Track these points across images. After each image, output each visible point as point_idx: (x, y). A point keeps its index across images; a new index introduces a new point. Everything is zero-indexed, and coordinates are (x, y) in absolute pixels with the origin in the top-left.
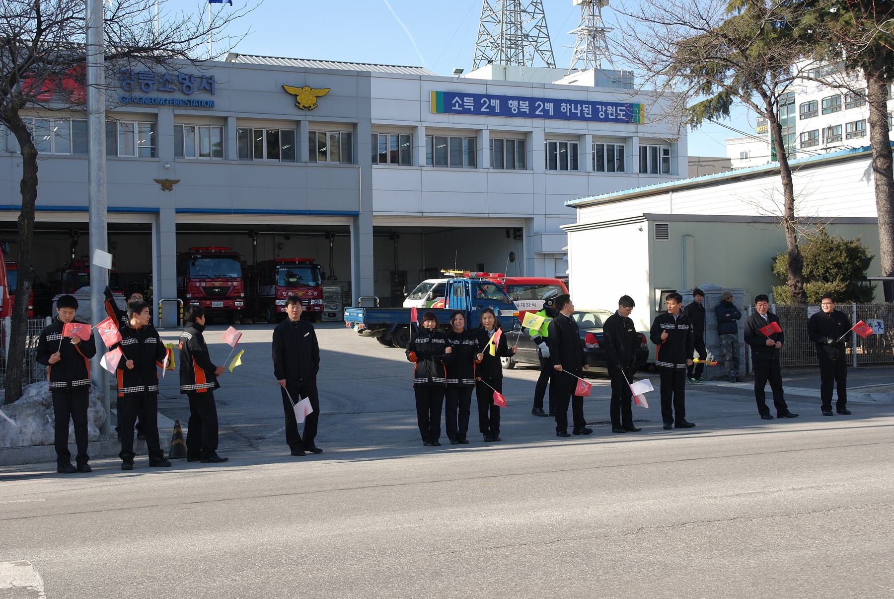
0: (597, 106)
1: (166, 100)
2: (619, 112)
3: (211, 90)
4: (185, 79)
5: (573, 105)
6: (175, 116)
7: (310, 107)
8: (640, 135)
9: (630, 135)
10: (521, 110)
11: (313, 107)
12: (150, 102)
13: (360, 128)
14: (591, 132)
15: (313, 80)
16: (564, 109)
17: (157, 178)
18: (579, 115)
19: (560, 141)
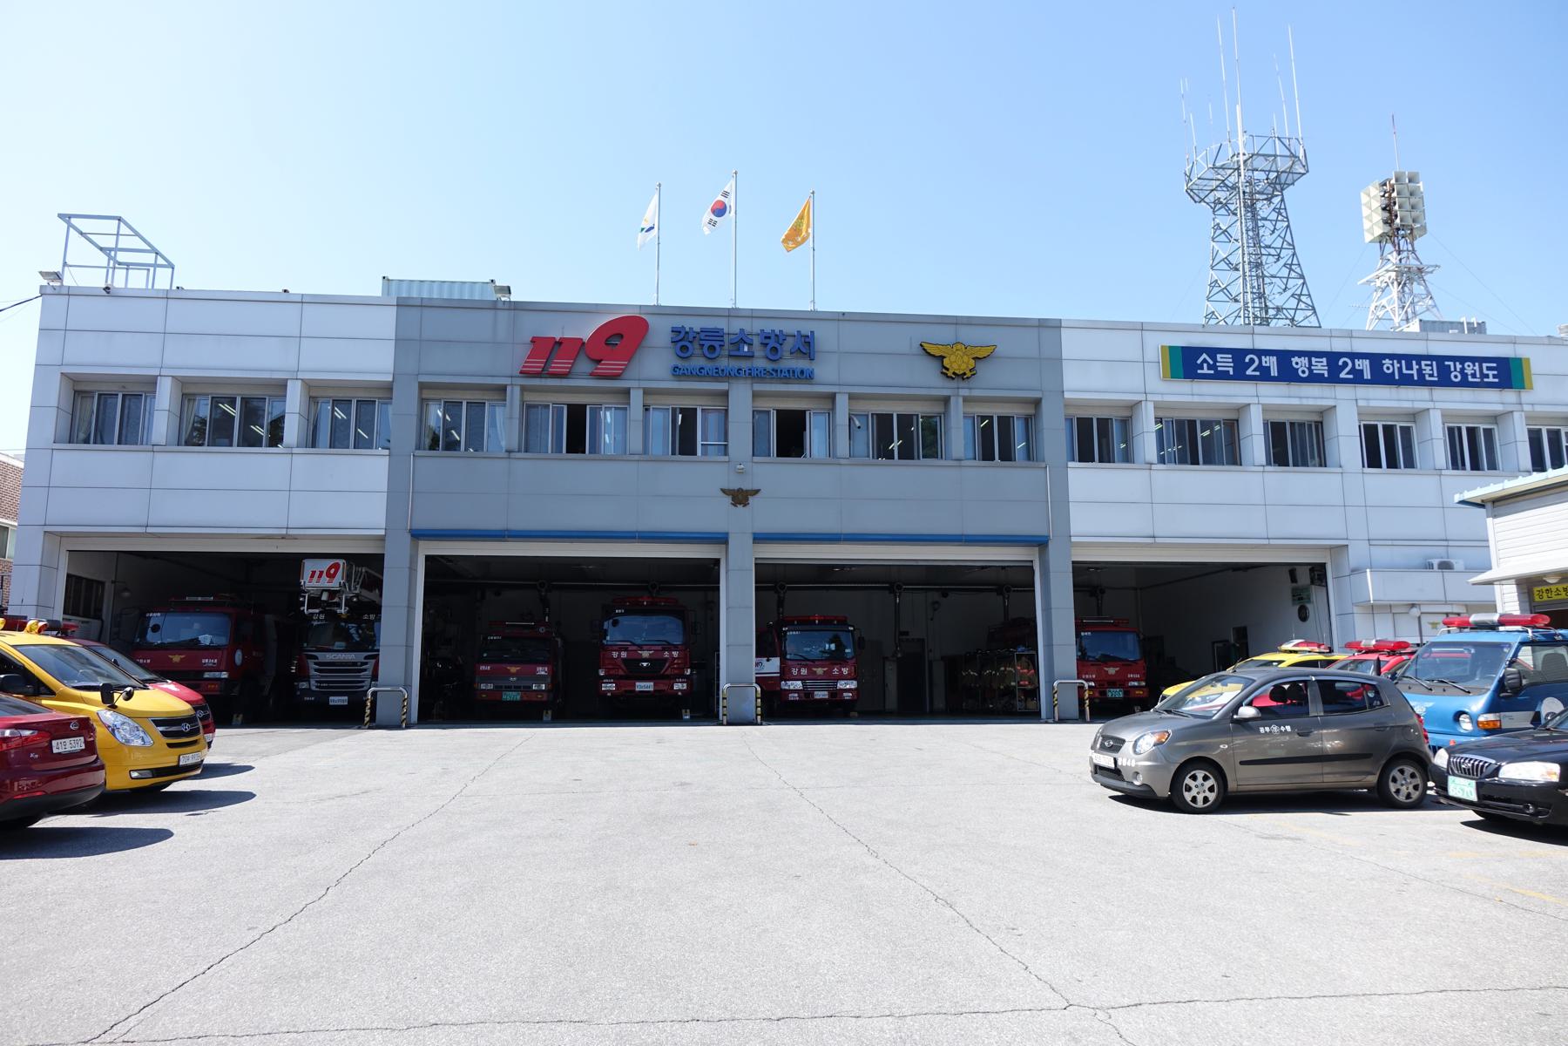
0: (1447, 363)
1: (741, 369)
4: (769, 338)
5: (1403, 362)
6: (756, 395)
7: (965, 374)
8: (1526, 408)
9: (1510, 408)
10: (1315, 372)
11: (969, 374)
12: (716, 373)
13: (1046, 407)
14: (1438, 405)
15: (969, 336)
16: (1388, 368)
17: (726, 487)
18: (1416, 378)
19: (1384, 423)
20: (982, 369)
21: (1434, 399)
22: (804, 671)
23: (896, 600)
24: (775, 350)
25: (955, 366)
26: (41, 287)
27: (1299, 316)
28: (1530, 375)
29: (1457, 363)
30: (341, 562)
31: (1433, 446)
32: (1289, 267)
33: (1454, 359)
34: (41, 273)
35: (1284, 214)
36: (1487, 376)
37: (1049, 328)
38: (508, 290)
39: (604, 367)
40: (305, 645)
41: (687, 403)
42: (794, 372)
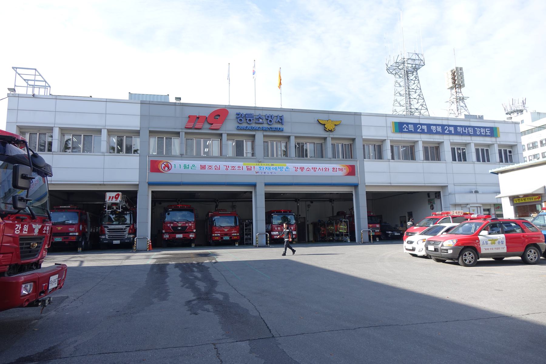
0: (476, 128)
2: (487, 131)
3: (282, 122)
4: (269, 117)
5: (463, 128)
6: (264, 136)
7: (332, 130)
8: (498, 143)
9: (493, 143)
10: (438, 131)
11: (333, 130)
13: (357, 141)
14: (473, 142)
15: (333, 118)
16: (459, 130)
18: (467, 133)
20: (337, 128)
21: (472, 139)
22: (279, 228)
23: (297, 204)
24: (271, 121)
25: (329, 128)
26: (8, 94)
27: (422, 112)
28: (499, 132)
29: (479, 129)
30: (120, 193)
31: (472, 154)
32: (419, 95)
33: (478, 127)
34: (8, 89)
35: (418, 78)
36: (487, 133)
37: (357, 115)
38: (180, 99)
39: (214, 126)
40: (103, 223)
41: (240, 139)
42: (277, 128)
